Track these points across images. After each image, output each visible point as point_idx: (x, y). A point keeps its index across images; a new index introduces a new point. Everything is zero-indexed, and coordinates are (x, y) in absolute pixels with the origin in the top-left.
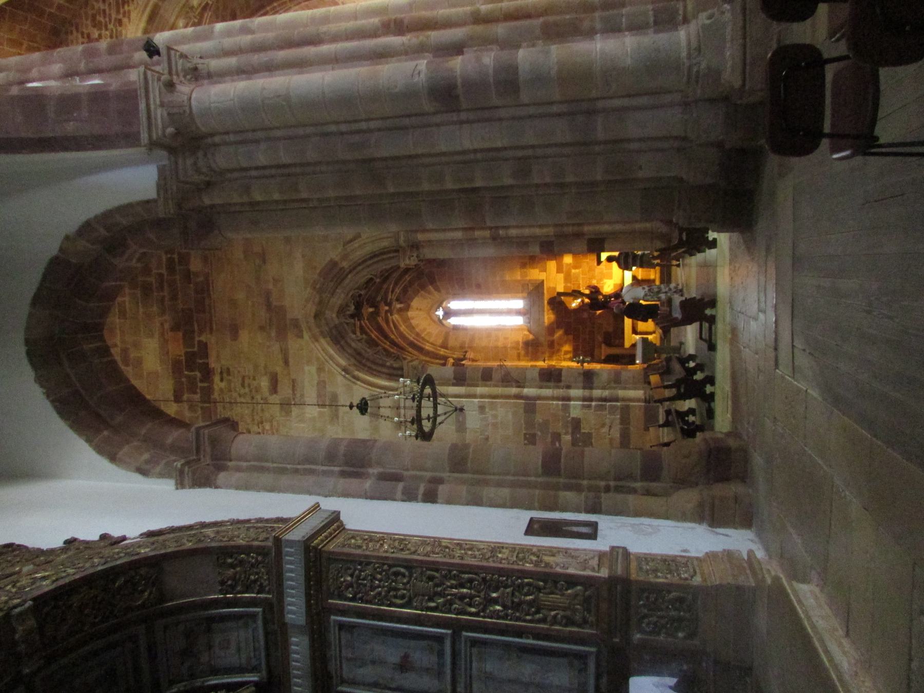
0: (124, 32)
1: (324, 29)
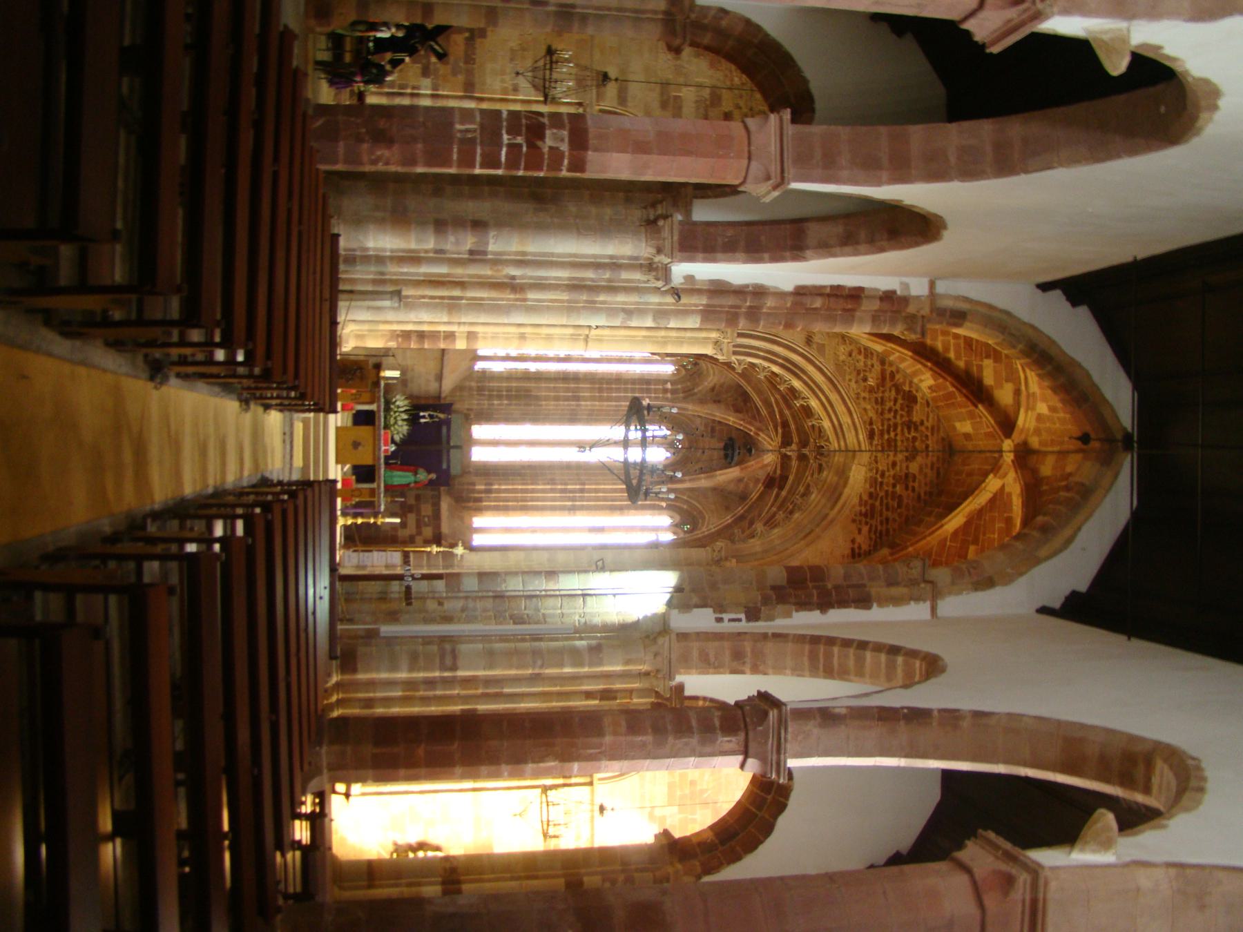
0: (868, 486)
1: (565, 296)
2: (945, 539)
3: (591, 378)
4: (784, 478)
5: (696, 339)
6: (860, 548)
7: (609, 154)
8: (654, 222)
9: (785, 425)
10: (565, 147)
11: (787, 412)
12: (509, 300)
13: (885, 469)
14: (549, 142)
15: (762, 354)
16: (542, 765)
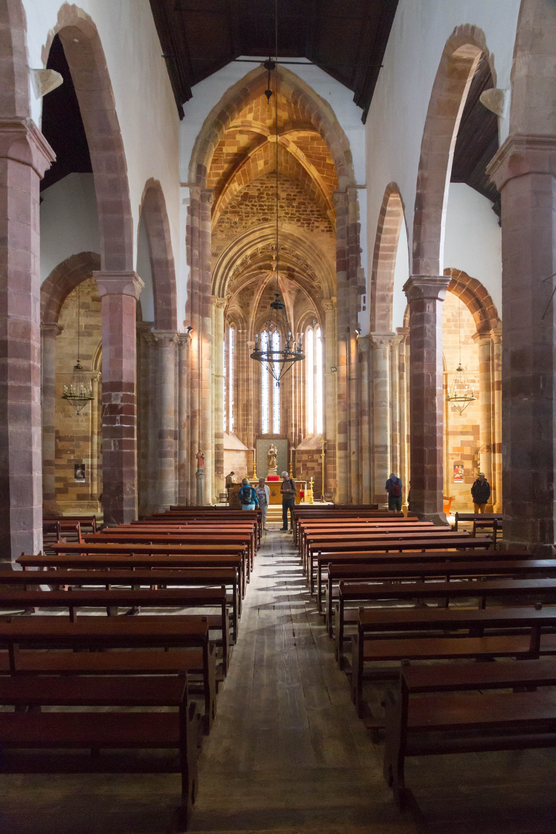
0: (293, 222)
2: (322, 177)
3: (237, 372)
4: (289, 269)
5: (216, 318)
6: (326, 227)
7: (124, 371)
8: (156, 343)
9: (260, 268)
10: (121, 394)
11: (253, 267)
12: (199, 419)
13: (284, 212)
14: (118, 402)
15: (223, 282)
16: (437, 406)
